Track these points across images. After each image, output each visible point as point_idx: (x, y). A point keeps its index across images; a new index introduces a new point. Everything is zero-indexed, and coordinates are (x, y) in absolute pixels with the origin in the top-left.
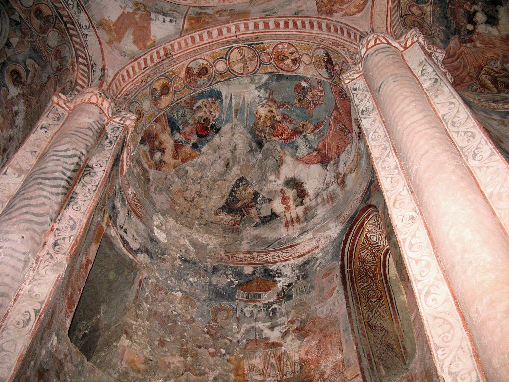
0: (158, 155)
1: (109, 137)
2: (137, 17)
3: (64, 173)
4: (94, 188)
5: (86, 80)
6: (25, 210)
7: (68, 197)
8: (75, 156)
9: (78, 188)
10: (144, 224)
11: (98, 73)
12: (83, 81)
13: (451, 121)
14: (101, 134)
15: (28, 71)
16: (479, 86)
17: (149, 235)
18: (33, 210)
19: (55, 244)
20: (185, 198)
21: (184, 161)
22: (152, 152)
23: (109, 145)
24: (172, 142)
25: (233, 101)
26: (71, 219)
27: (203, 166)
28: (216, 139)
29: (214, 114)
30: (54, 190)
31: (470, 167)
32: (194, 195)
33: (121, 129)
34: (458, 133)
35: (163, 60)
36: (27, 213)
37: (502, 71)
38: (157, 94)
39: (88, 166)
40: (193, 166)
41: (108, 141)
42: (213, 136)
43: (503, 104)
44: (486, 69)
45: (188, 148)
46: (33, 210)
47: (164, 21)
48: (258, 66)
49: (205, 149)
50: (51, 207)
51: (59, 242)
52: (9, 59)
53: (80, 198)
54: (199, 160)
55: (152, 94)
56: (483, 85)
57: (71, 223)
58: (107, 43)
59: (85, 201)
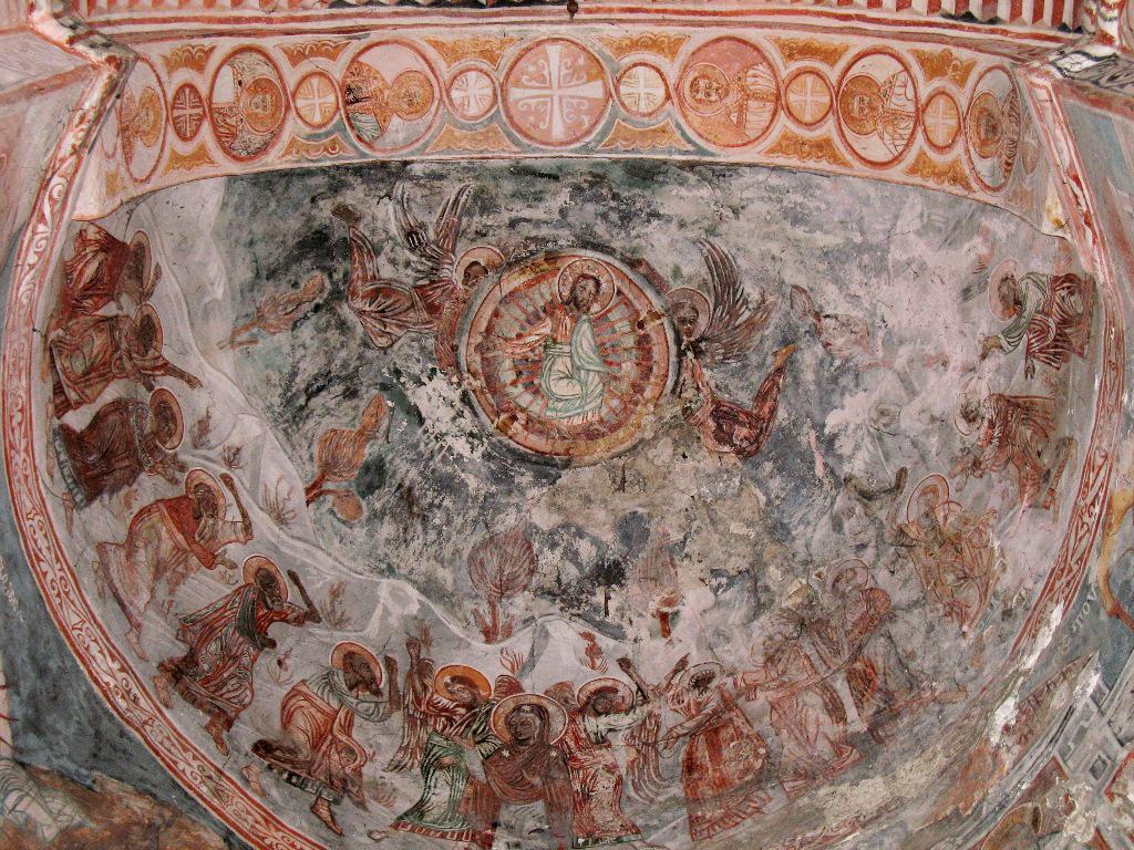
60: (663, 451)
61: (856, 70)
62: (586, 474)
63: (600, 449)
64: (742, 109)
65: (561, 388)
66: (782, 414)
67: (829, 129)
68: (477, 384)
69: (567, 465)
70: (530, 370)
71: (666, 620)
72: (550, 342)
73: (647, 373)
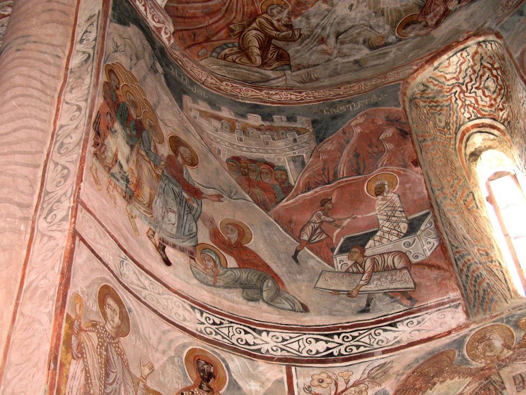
13: (61, 140)
16: (235, 49)
31: (36, 230)
34: (56, 164)
37: (284, 28)
43: (257, 88)
44: (262, 20)
56: (244, 51)
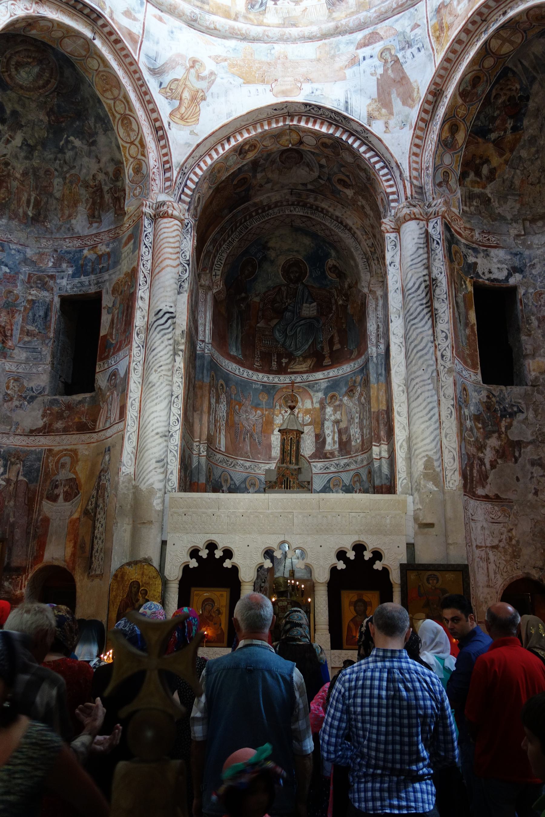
0: (485, 170)
1: (434, 237)
2: (390, 72)
3: (422, 305)
4: (445, 296)
5: (392, 182)
6: (415, 351)
7: (433, 315)
8: (421, 284)
9: (436, 305)
10: (502, 248)
11: (397, 174)
12: (391, 186)
14: (427, 241)
15: (348, 176)
17: (511, 253)
18: (419, 348)
19: (442, 356)
20: (532, 184)
21: (512, 151)
22: (478, 174)
23: (437, 246)
24: (491, 145)
25: (525, 63)
26: (443, 331)
27: (533, 140)
28: (531, 105)
29: (514, 88)
30: (423, 322)
32: (537, 174)
33: (438, 222)
35: (436, 102)
36: (417, 352)
38: (450, 140)
39: (434, 280)
40: (523, 147)
41: (435, 242)
42: (526, 105)
45: (509, 136)
46: (419, 348)
47: (413, 56)
48: (524, 35)
49: (526, 122)
50: (428, 336)
51: (444, 353)
52: (329, 174)
53: (441, 311)
54: (526, 138)
55: (446, 146)
57: (444, 335)
58: (385, 132)
59: (444, 312)
60: (33, 105)
61: (131, 118)
62: (14, 95)
63: (21, 92)
64: (107, 90)
65: (23, 74)
66: (64, 124)
67: (118, 116)
68: (5, 60)
69: (11, 90)
70: (19, 65)
71: (8, 142)
72: (28, 63)
73: (44, 87)
